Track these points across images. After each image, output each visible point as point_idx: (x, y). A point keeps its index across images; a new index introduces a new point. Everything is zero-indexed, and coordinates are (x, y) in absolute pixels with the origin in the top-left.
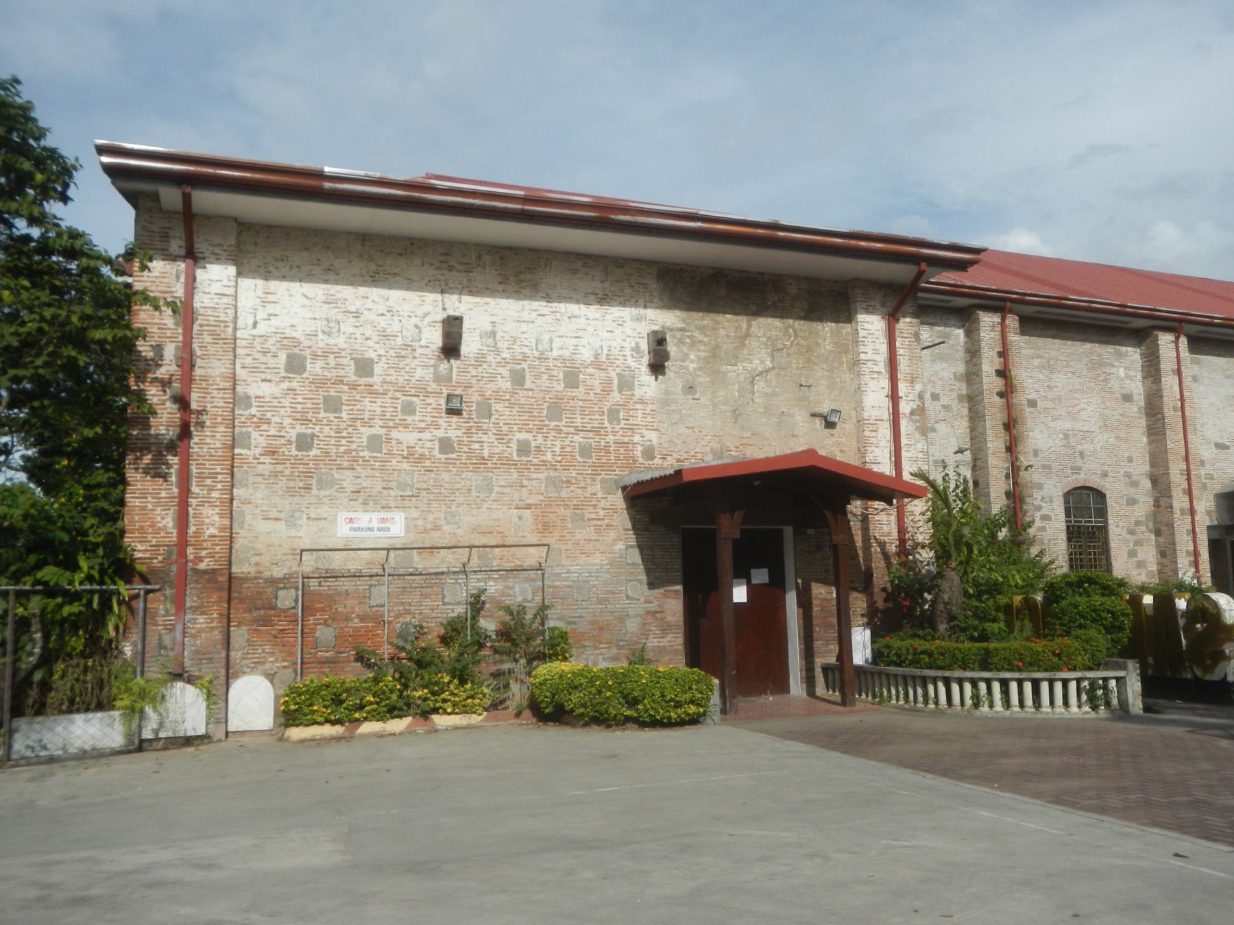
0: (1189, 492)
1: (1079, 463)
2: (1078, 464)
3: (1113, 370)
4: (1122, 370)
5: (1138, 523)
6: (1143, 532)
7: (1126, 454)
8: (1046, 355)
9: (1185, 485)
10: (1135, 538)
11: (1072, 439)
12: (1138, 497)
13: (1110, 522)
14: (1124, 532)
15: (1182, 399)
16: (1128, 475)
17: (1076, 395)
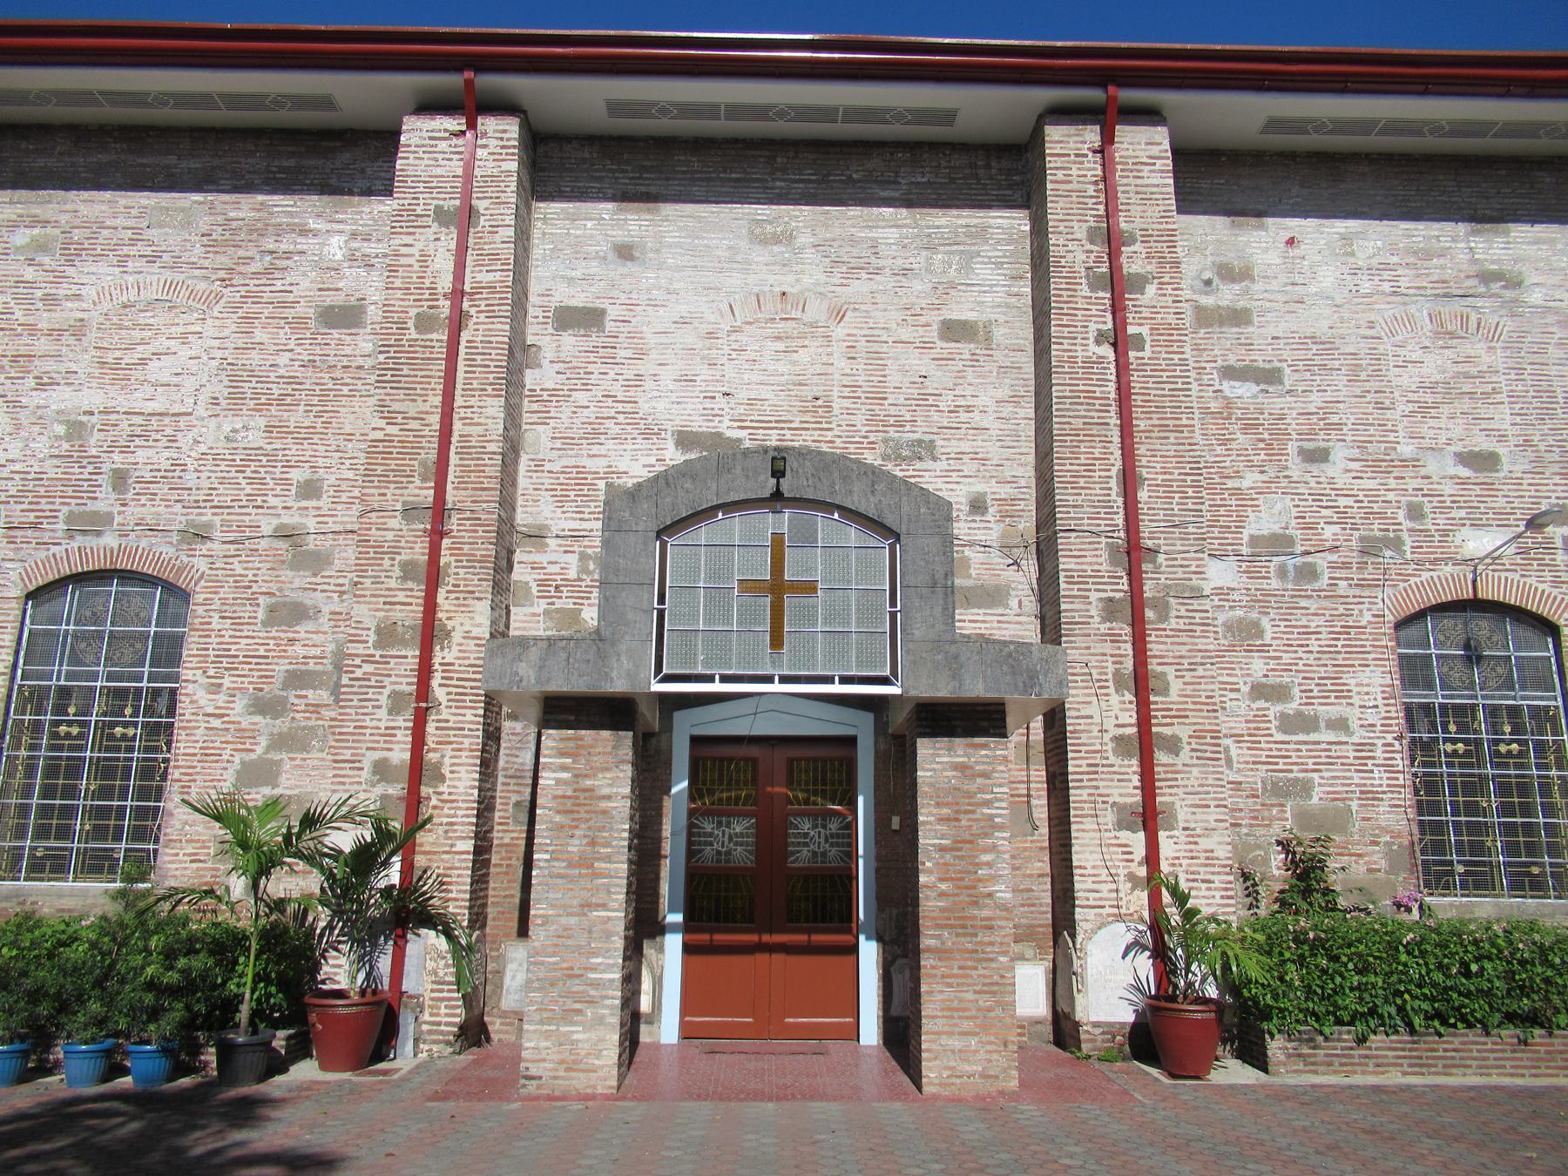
0: (433, 577)
1: (105, 501)
2: (100, 506)
3: (304, 243)
4: (336, 241)
5: (298, 679)
6: (316, 708)
7: (297, 475)
8: (64, 218)
9: (418, 552)
10: (282, 724)
11: (97, 435)
12: (308, 599)
13: (186, 674)
14: (240, 705)
15: (457, 294)
16: (286, 534)
17: (144, 318)
